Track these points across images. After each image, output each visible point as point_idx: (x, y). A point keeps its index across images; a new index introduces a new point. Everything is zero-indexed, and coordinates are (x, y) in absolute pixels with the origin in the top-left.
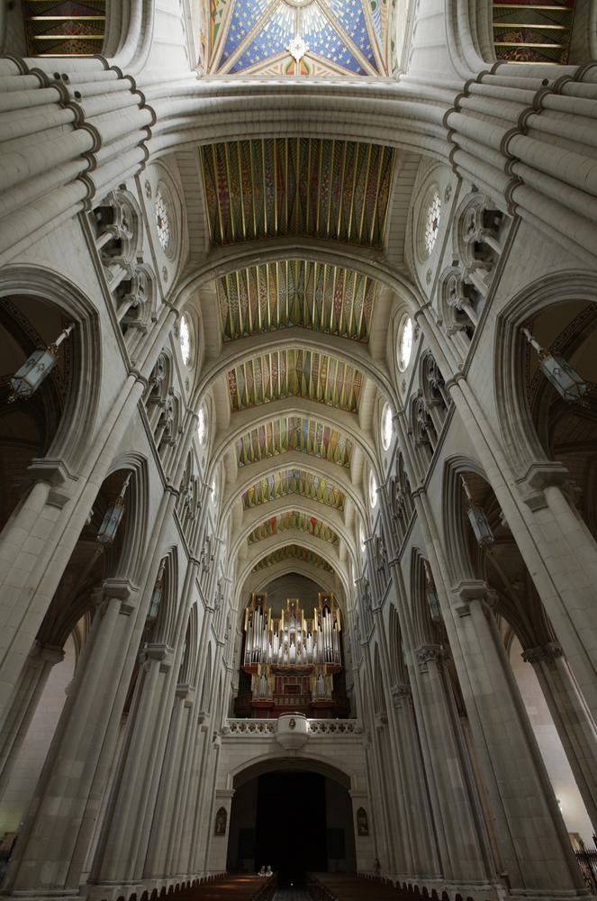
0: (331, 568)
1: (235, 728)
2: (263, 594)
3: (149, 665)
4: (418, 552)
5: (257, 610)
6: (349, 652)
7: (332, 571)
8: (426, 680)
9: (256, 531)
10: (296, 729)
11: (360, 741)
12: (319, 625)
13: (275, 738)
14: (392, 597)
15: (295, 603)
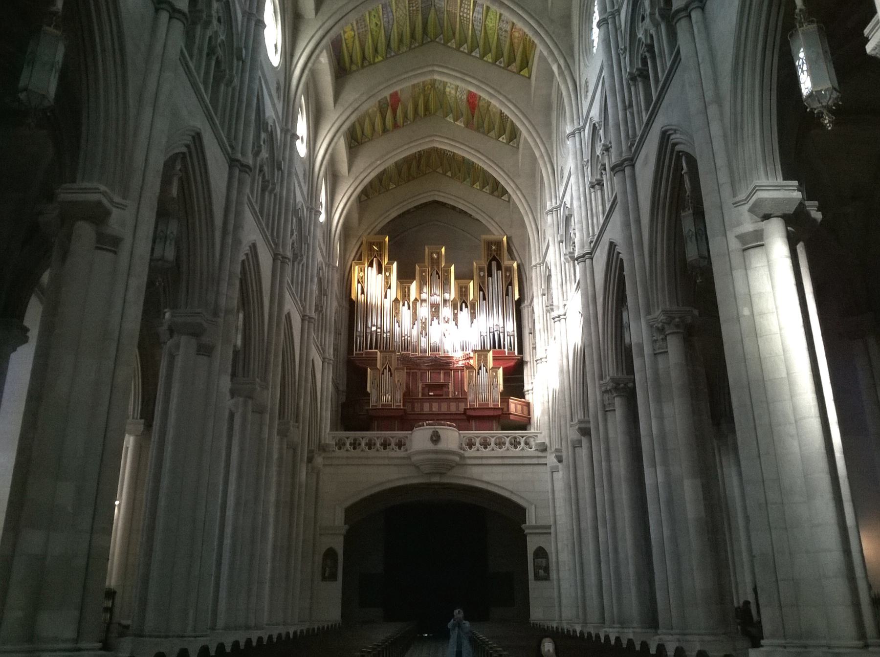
0: (505, 192)
1: (344, 444)
2: (378, 239)
3: (177, 346)
4: (675, 138)
5: (371, 265)
6: (532, 332)
7: (505, 198)
8: (661, 366)
9: (360, 121)
10: (442, 446)
11: (542, 461)
12: (481, 289)
13: (409, 458)
14: (615, 233)
15: (439, 254)
